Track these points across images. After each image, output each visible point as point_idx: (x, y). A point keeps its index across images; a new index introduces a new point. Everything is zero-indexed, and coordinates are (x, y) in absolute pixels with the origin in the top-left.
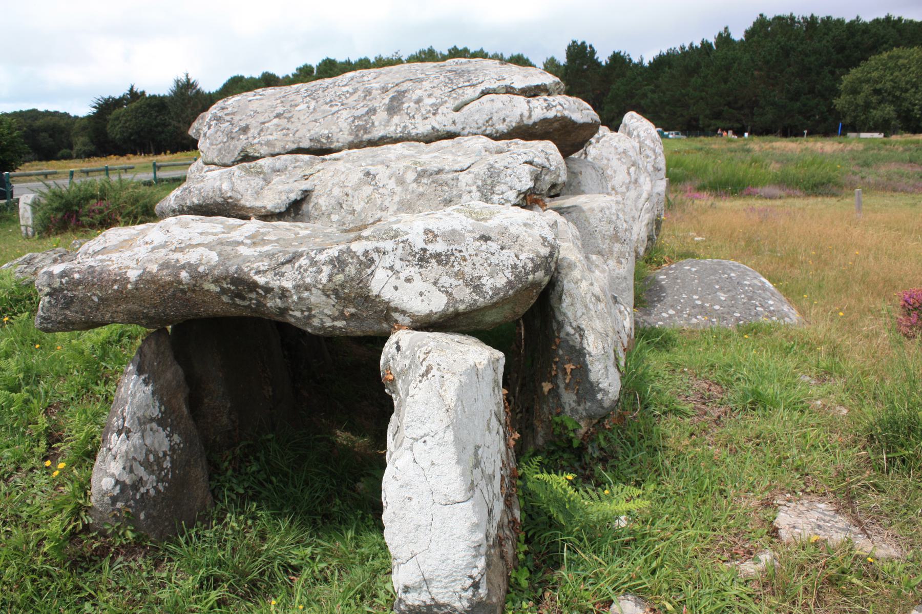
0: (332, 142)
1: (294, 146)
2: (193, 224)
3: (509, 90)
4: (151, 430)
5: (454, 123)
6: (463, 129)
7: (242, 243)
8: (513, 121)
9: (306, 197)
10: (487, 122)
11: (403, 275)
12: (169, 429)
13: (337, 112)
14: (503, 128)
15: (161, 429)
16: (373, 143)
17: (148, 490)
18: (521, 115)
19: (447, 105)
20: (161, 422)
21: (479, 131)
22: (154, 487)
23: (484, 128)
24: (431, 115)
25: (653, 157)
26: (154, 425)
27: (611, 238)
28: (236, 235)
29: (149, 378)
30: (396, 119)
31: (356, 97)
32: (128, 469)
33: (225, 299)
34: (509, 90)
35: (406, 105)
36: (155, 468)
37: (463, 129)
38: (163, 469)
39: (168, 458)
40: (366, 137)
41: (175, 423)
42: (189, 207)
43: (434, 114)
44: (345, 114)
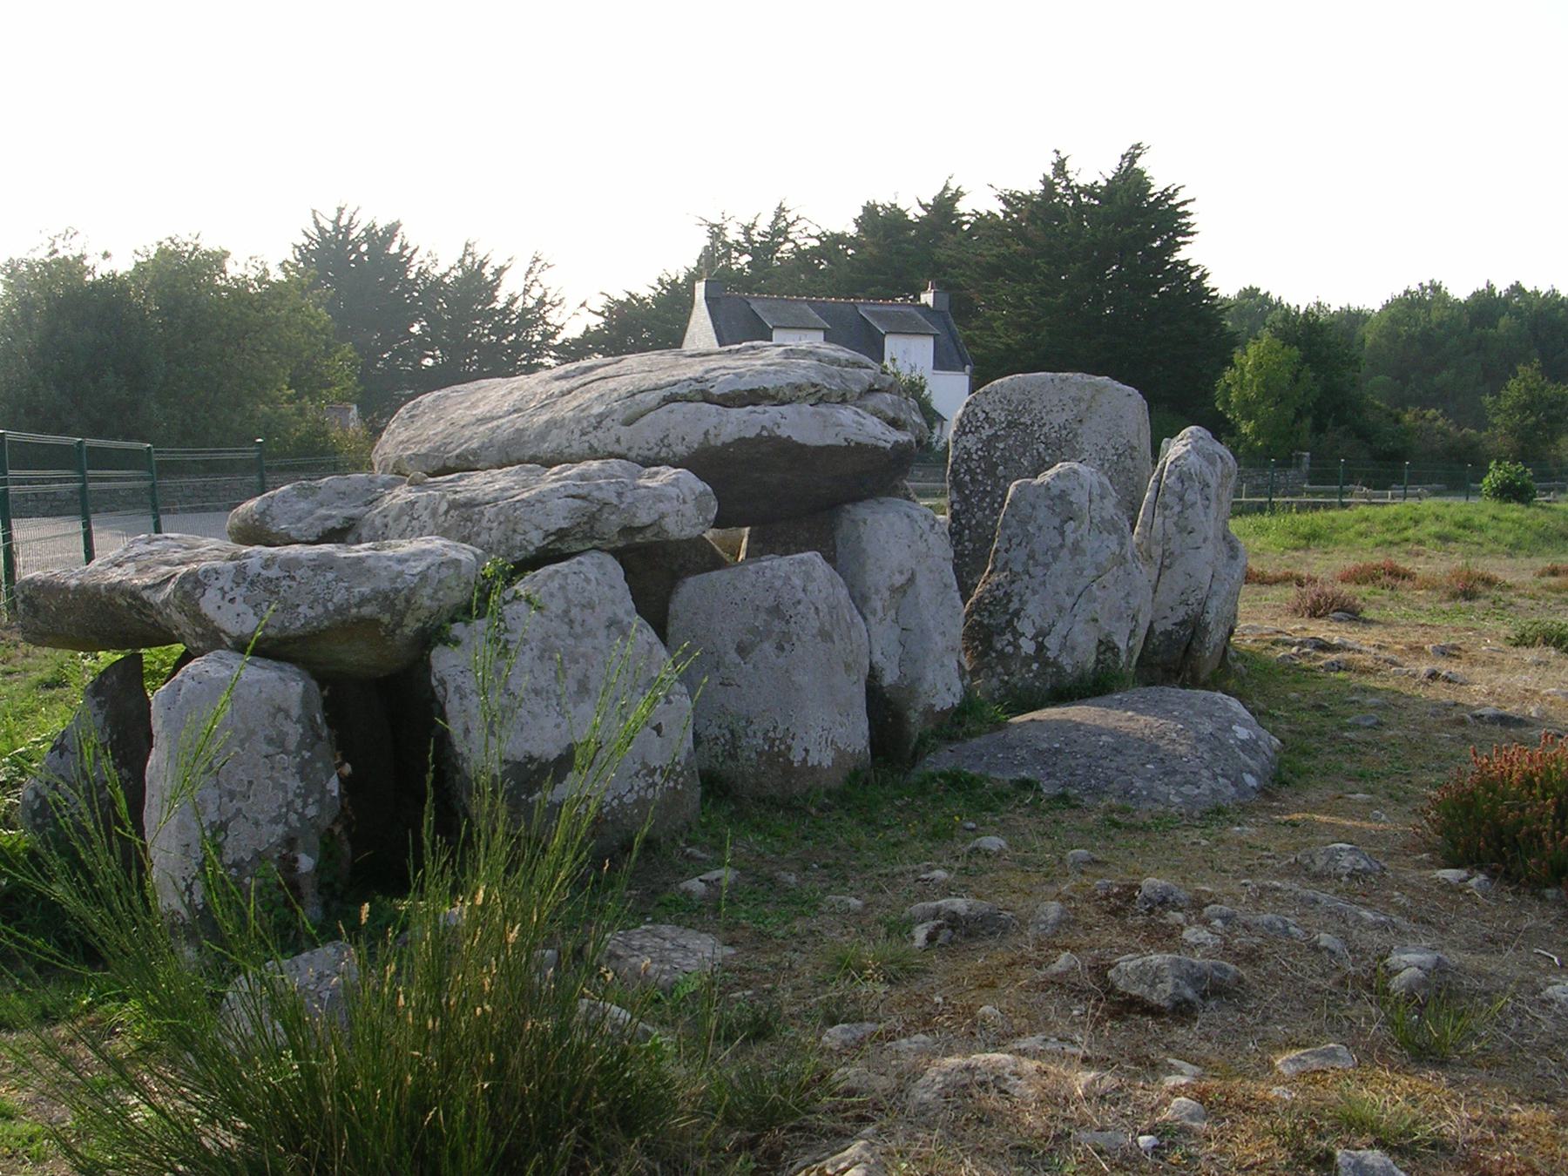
5: (618, 441)
6: (629, 449)
11: (228, 597)
18: (706, 433)
23: (656, 449)
25: (1177, 509)
27: (769, 611)
43: (595, 428)
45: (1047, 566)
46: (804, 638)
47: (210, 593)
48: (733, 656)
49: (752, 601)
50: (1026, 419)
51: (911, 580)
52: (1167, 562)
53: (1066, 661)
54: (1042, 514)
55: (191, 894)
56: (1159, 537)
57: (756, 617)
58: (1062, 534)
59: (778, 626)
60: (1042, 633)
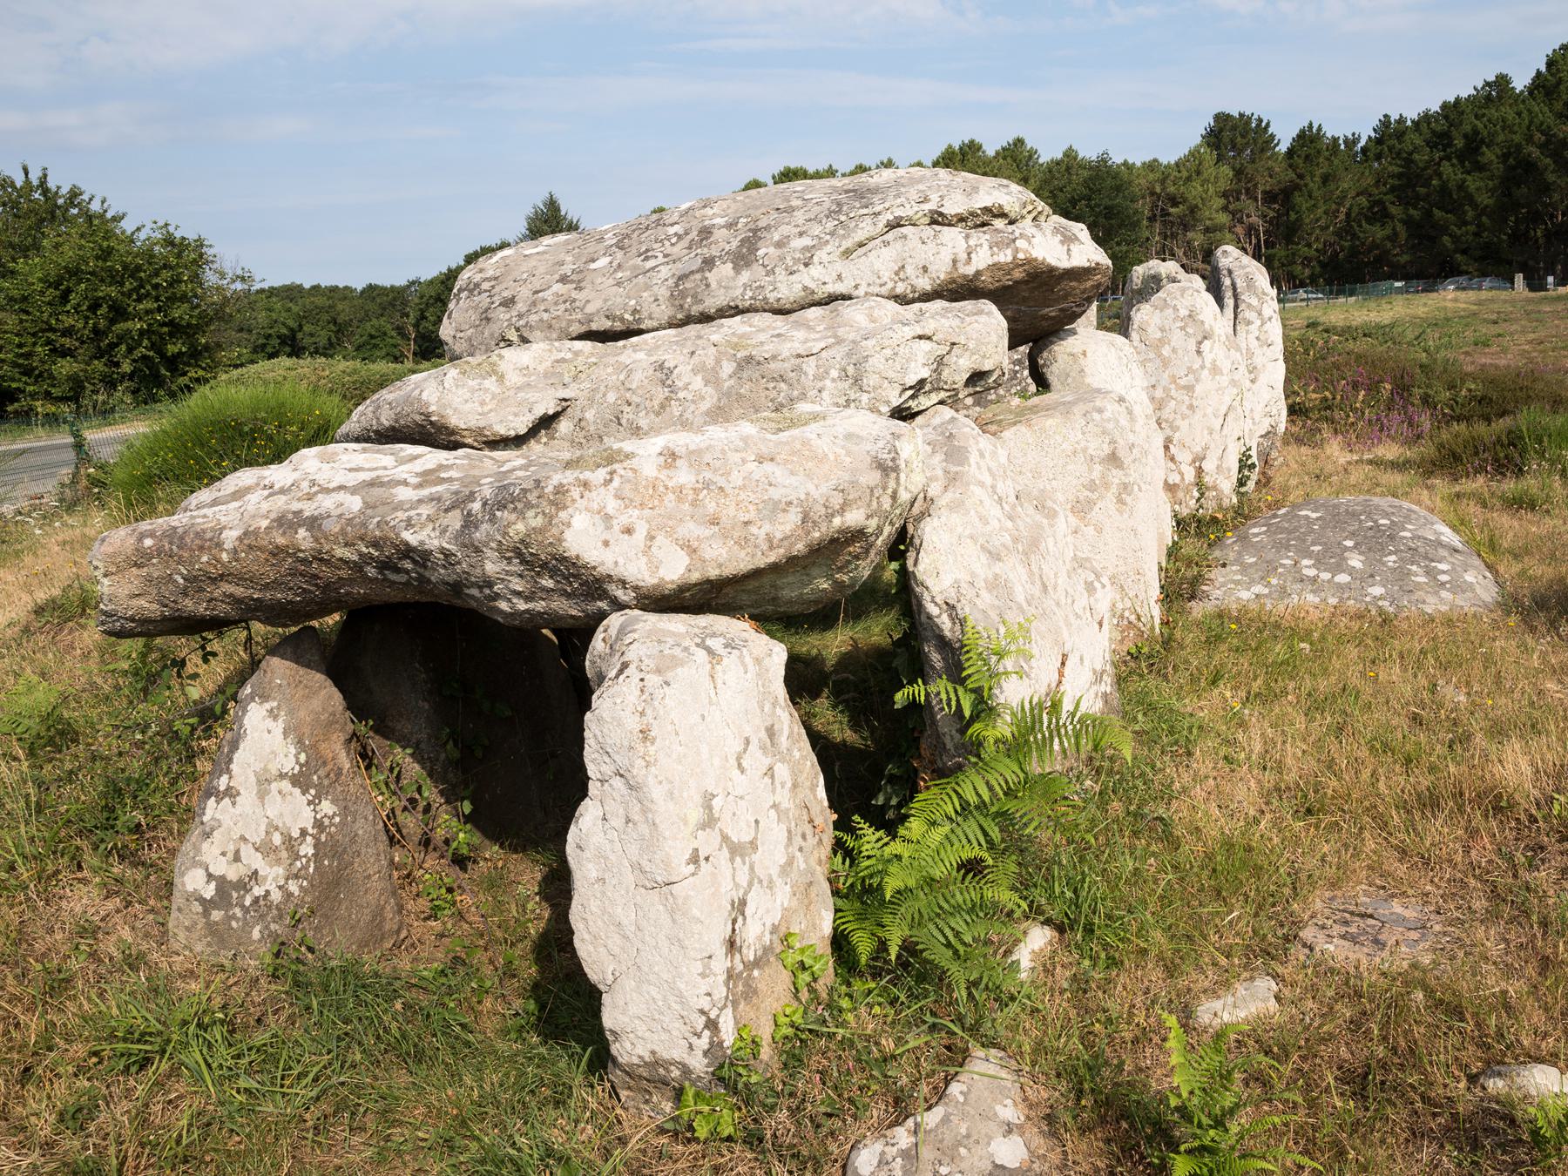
0: (639, 321)
1: (583, 329)
2: (344, 458)
3: (938, 219)
5: (839, 277)
6: (856, 287)
7: (405, 483)
8: (941, 271)
9: (564, 410)
10: (897, 274)
12: (313, 792)
13: (653, 268)
14: (925, 284)
15: (297, 791)
16: (705, 318)
17: (268, 892)
19: (829, 248)
20: (300, 781)
21: (884, 291)
22: (280, 888)
23: (890, 285)
24: (802, 267)
25: (1259, 322)
26: (286, 785)
28: (403, 472)
29: (278, 708)
30: (745, 276)
31: (685, 242)
32: (230, 856)
33: (371, 572)
34: (938, 219)
35: (760, 253)
36: (284, 854)
37: (856, 287)
38: (298, 857)
39: (309, 839)
40: (695, 310)
41: (326, 782)
42: (377, 432)
43: (806, 265)
44: (665, 271)
45: (1189, 389)
49: (1085, 450)
54: (1177, 338)
57: (1091, 470)
58: (1199, 352)
59: (1116, 477)
60: (1198, 460)
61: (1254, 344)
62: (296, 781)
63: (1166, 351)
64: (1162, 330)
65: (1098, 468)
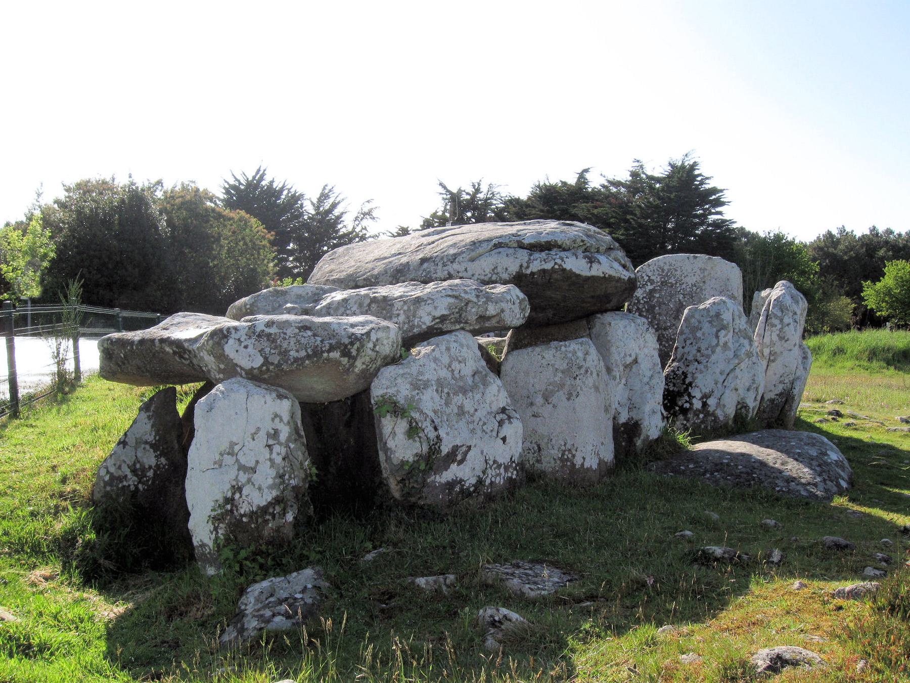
4: (144, 448)
5: (466, 270)
10: (493, 270)
11: (243, 345)
14: (505, 276)
15: (152, 450)
20: (154, 447)
23: (490, 275)
25: (779, 326)
26: (148, 447)
43: (452, 262)
45: (708, 357)
46: (584, 389)
47: (231, 342)
48: (539, 400)
50: (672, 281)
51: (636, 361)
52: (772, 358)
53: (719, 413)
54: (706, 326)
55: (217, 532)
56: (768, 343)
57: (555, 376)
58: (717, 337)
60: (705, 397)
61: (775, 338)
62: (152, 446)
63: (699, 334)
64: (700, 322)
65: (560, 375)
